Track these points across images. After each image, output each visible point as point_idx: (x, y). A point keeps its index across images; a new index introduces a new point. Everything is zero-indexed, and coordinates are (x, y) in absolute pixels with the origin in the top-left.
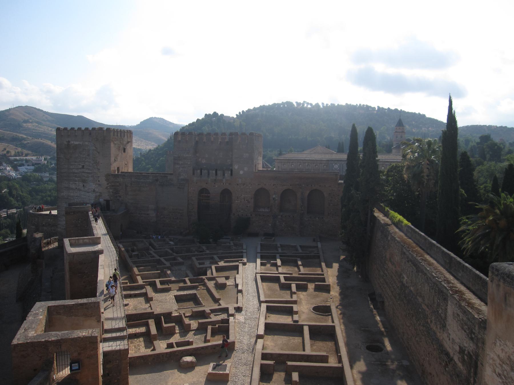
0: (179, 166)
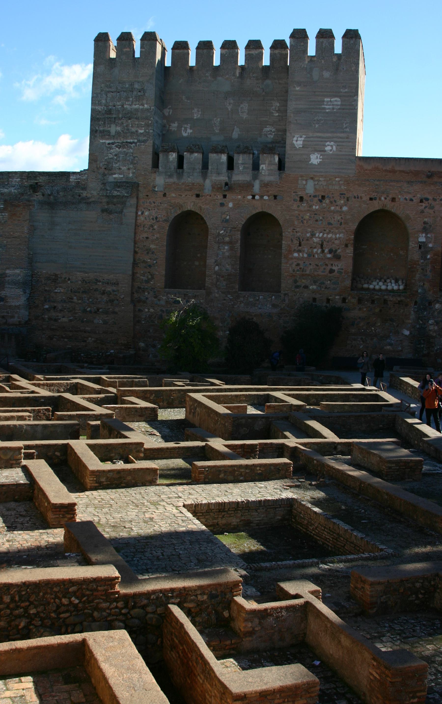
0: (108, 142)
